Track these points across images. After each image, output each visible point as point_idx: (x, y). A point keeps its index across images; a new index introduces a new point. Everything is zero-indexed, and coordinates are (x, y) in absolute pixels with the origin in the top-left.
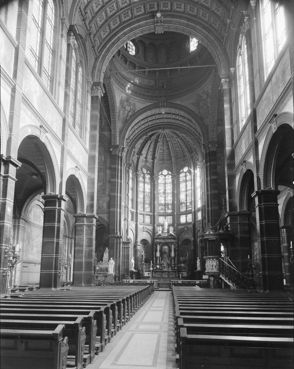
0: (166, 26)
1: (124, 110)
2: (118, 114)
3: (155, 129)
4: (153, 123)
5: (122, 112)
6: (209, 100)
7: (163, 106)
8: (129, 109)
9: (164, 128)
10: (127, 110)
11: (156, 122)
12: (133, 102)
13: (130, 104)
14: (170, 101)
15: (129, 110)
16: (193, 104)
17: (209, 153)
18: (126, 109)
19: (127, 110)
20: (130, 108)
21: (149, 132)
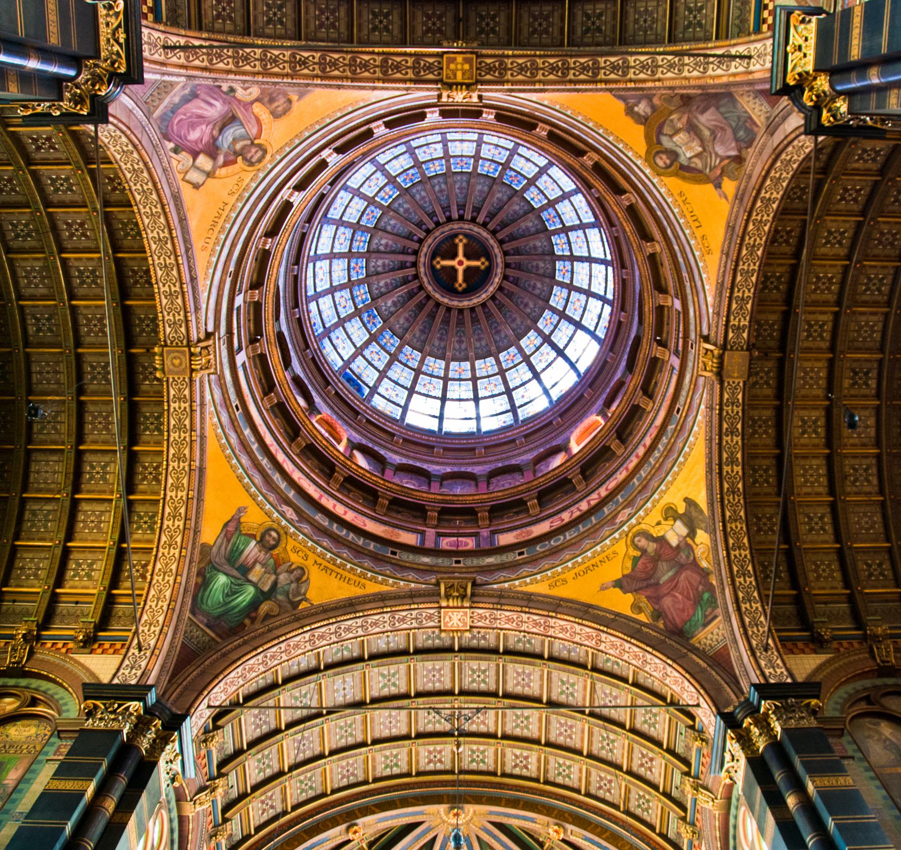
0: (489, 61)
1: (239, 575)
2: (200, 580)
3: (405, 802)
4: (396, 771)
5: (222, 579)
6: (702, 537)
7: (456, 594)
8: (270, 583)
9: (456, 801)
10: (255, 585)
11: (410, 763)
12: (295, 559)
13: (277, 565)
14: (495, 586)
15: (266, 588)
16: (618, 584)
17: (775, 746)
18: (253, 576)
19: (255, 585)
20: (273, 577)
21: (366, 811)
